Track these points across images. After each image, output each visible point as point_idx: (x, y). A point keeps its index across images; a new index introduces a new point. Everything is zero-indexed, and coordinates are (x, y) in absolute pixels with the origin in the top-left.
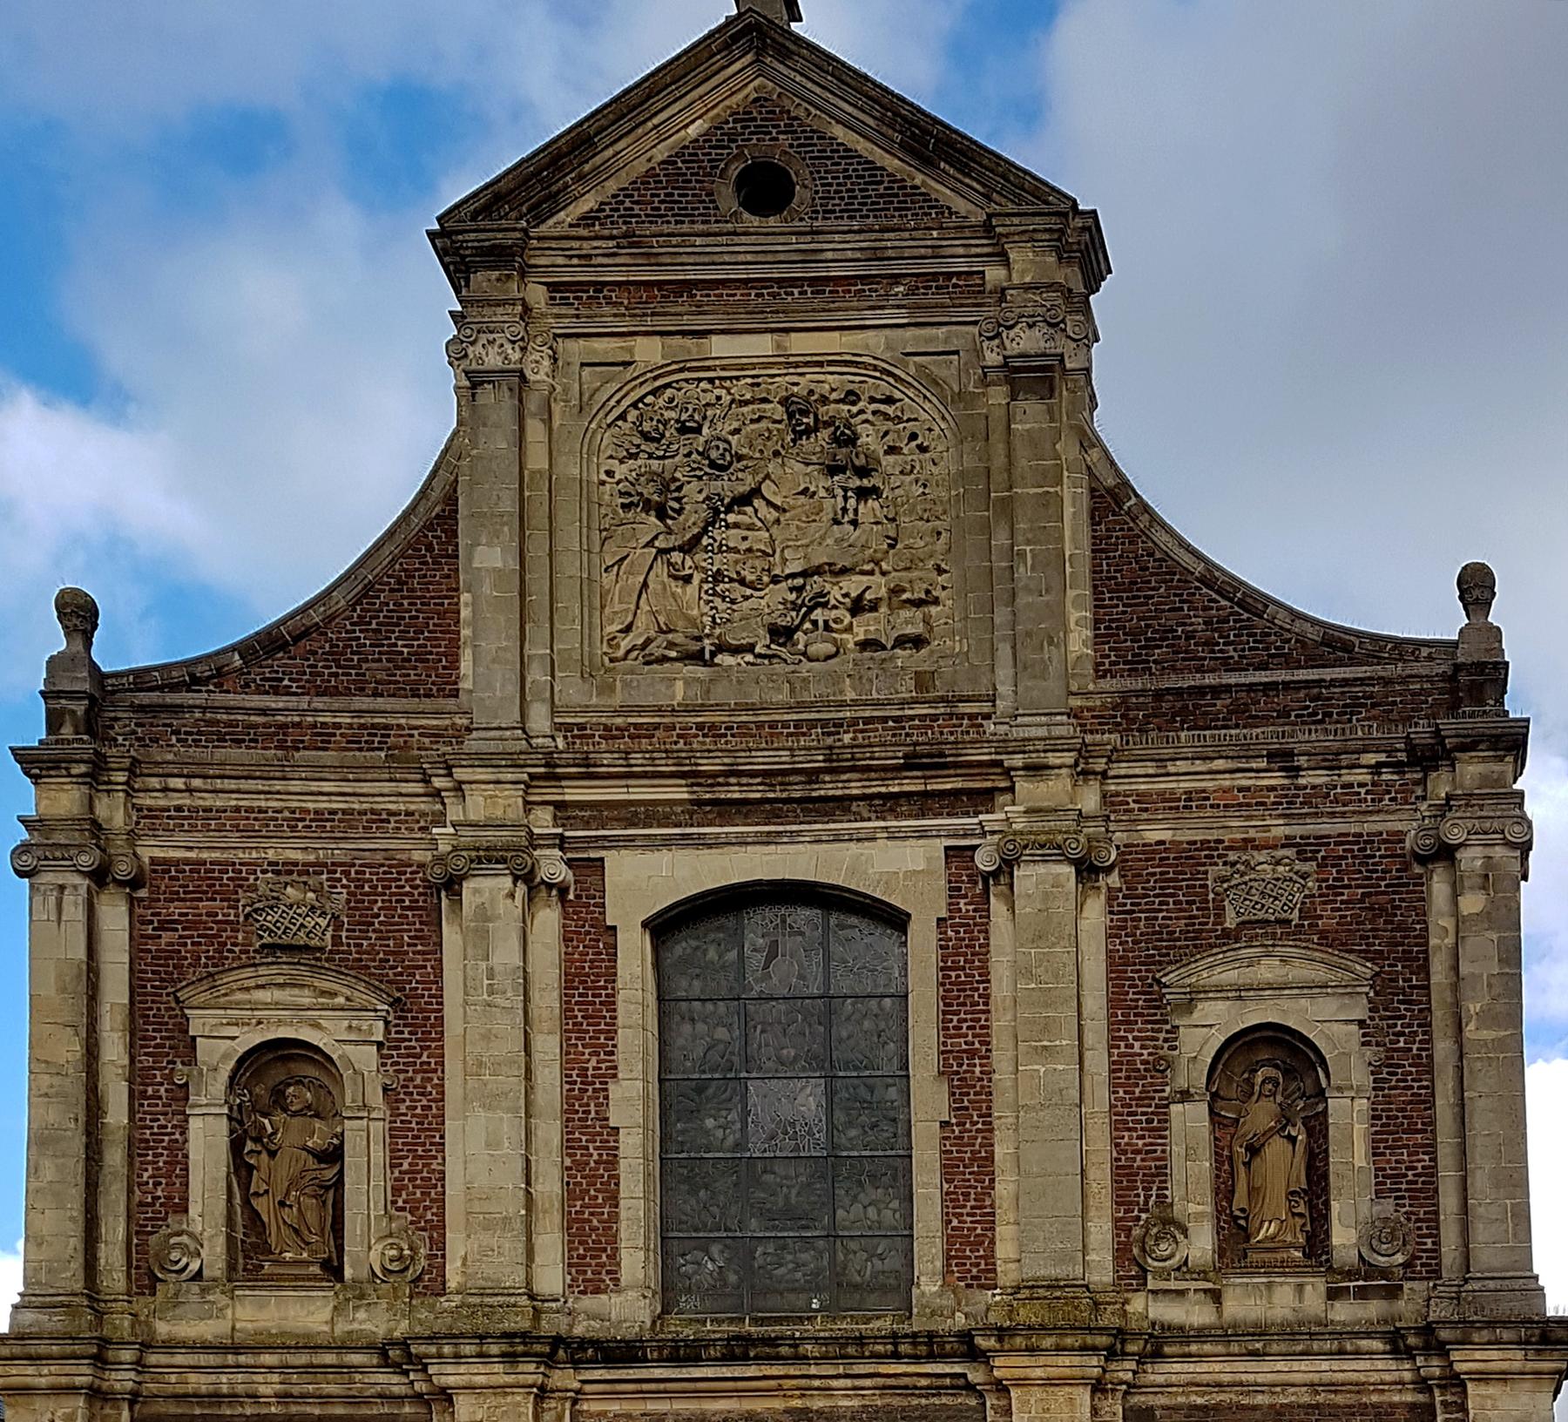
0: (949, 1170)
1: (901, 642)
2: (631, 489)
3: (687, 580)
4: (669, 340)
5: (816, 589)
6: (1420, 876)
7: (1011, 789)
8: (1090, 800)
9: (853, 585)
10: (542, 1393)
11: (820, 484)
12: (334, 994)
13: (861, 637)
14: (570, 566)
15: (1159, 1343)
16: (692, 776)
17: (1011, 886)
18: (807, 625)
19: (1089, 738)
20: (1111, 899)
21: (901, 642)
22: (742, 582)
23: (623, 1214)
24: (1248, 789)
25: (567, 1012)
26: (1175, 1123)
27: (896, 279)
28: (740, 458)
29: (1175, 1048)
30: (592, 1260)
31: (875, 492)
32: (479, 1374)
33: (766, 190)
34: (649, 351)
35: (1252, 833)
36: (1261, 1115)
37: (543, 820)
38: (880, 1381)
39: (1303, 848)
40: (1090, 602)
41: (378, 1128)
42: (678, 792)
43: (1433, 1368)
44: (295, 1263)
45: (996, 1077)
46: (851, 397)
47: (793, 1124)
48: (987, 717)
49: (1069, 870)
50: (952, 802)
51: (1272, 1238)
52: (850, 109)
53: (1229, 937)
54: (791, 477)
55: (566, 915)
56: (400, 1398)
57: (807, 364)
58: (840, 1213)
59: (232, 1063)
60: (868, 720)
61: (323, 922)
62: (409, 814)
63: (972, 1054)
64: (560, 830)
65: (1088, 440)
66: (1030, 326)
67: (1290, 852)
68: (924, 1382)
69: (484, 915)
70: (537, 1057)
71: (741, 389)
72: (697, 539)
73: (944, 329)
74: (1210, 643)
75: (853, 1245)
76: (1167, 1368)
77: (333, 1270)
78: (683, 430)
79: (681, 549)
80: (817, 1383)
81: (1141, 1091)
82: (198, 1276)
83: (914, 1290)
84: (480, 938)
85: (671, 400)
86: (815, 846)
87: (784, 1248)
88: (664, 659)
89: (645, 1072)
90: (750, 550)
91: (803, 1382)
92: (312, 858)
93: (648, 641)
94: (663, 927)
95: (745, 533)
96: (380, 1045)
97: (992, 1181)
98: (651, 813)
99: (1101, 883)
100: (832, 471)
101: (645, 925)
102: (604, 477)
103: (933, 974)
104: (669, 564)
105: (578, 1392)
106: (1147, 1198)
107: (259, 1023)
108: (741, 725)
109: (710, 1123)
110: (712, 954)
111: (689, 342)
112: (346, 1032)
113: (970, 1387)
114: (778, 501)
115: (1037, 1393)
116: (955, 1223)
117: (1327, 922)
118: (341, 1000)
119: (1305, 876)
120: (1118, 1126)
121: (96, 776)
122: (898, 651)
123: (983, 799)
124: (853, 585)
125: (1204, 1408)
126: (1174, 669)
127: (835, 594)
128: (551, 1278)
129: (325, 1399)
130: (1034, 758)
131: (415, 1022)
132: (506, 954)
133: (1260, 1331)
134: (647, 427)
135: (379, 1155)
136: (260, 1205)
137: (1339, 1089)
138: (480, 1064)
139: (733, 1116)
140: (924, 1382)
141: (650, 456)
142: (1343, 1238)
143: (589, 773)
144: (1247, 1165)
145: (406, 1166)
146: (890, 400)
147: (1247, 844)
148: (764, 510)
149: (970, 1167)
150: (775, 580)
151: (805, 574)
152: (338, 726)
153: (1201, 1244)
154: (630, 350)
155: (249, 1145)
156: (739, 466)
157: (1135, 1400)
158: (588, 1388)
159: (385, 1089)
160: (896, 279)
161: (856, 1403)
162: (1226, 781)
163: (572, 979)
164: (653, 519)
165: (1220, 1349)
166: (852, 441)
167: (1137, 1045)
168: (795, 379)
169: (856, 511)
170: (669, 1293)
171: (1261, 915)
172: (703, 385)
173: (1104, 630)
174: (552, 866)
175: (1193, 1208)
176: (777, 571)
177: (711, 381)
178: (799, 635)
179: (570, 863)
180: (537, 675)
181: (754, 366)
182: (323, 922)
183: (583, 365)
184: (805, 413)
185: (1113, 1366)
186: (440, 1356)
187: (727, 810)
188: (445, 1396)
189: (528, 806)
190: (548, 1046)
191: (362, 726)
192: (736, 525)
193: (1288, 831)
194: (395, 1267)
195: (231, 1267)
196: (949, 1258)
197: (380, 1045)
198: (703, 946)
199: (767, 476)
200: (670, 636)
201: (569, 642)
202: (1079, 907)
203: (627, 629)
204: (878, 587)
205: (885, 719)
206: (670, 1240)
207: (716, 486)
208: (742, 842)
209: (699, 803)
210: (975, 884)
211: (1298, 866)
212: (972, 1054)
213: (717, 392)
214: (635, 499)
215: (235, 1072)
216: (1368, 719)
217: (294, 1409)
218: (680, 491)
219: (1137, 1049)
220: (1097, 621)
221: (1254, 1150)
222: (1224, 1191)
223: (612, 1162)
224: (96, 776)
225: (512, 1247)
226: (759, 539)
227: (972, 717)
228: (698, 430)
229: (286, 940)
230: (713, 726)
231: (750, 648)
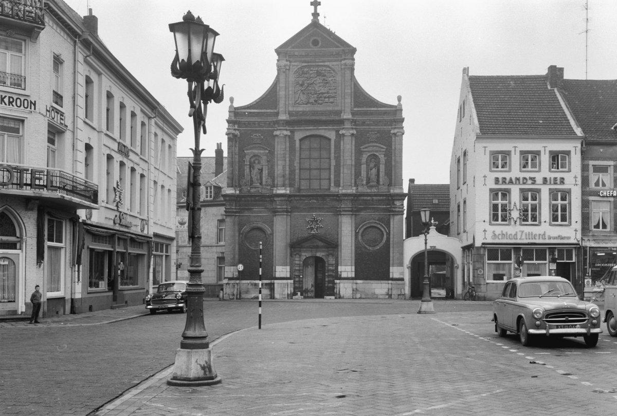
26: (362, 168)
33: (315, 43)
94: (301, 140)
124: (325, 95)
131: (272, 153)
151: (319, 94)
198: (307, 142)
210: (340, 137)
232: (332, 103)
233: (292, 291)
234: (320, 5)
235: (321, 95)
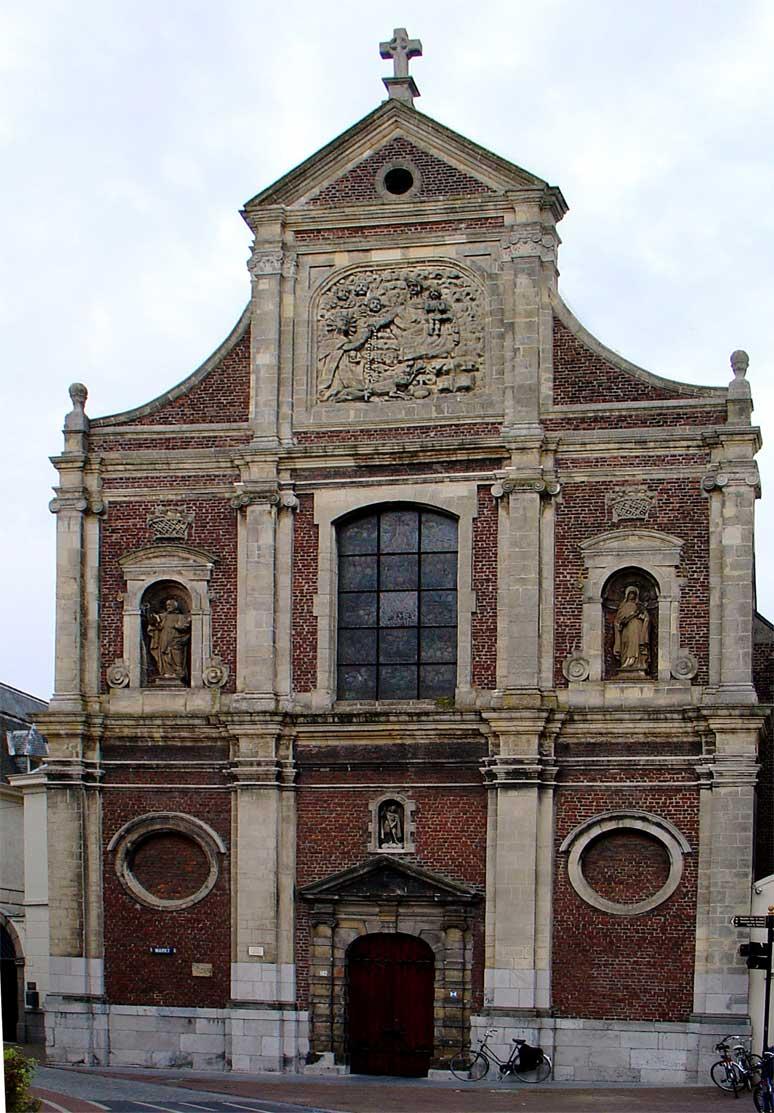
0: (475, 636)
1: (460, 389)
2: (331, 323)
3: (358, 363)
4: (351, 254)
5: (419, 366)
6: (706, 499)
7: (510, 458)
8: (549, 463)
9: (437, 364)
10: (279, 738)
11: (421, 316)
12: (188, 559)
13: (440, 387)
14: (303, 359)
15: (573, 714)
16: (355, 455)
17: (508, 503)
18: (415, 382)
19: (550, 434)
20: (558, 508)
21: (460, 389)
22: (384, 363)
23: (319, 655)
24: (625, 457)
25: (295, 564)
27: (460, 221)
28: (385, 306)
29: (586, 578)
30: (304, 678)
31: (448, 320)
32: (249, 729)
33: (399, 182)
34: (342, 260)
35: (627, 478)
36: (628, 609)
37: (286, 478)
38: (439, 732)
39: (652, 485)
40: (552, 370)
41: (207, 619)
42: (350, 463)
43: (701, 726)
44: (170, 679)
45: (499, 591)
46: (438, 277)
47: (401, 613)
48: (500, 423)
49: (537, 496)
50: (482, 464)
51: (631, 666)
52: (440, 142)
53: (615, 526)
54: (411, 312)
55: (295, 520)
56: (215, 739)
57: (418, 262)
58: (423, 654)
59: (142, 592)
60: (441, 426)
61: (184, 527)
62: (224, 476)
63: (488, 580)
64: (293, 482)
65: (552, 293)
66: (525, 243)
67: (645, 487)
68: (459, 732)
69: (257, 522)
70: (280, 586)
71: (386, 275)
72: (363, 344)
73: (483, 244)
74: (610, 388)
75: (429, 668)
76: (576, 726)
77: (186, 681)
78: (357, 295)
79: (355, 350)
80: (408, 733)
81: (569, 598)
82: (127, 686)
83: (457, 691)
84: (255, 533)
85: (352, 281)
86: (415, 486)
87: (396, 669)
88: (346, 400)
89: (331, 590)
90: (388, 349)
91: (402, 732)
92: (179, 498)
93: (338, 392)
94: (341, 524)
95: (385, 341)
96: (208, 581)
97: (496, 640)
98: (338, 472)
99: (553, 501)
100: (429, 312)
101: (332, 523)
102: (319, 318)
103: (470, 544)
104: (349, 357)
105: (296, 736)
106: (571, 647)
107: (155, 573)
108: (381, 430)
109: (362, 612)
110: (365, 535)
111: (361, 254)
112: (191, 575)
113: (482, 735)
114: (402, 326)
115: (512, 738)
116: (477, 659)
117: (663, 519)
118: (191, 561)
119: (651, 498)
120: (558, 613)
121: (86, 467)
122: (458, 393)
123: (497, 463)
124: (437, 364)
125: (593, 744)
126: (591, 400)
127: (429, 368)
128: (285, 684)
129: (183, 739)
130: (520, 445)
131: (224, 573)
132: (267, 538)
133: (619, 709)
134: (340, 294)
135: (207, 630)
136: (154, 653)
137: (665, 597)
138: (253, 590)
139: (374, 609)
141: (342, 307)
142: (663, 665)
143: (307, 455)
144: (621, 632)
145: (219, 635)
146: (457, 277)
147: (623, 483)
148: (395, 330)
149: (486, 634)
150: (400, 362)
151: (413, 359)
152: (193, 438)
153: (596, 668)
154: (333, 260)
155: (150, 627)
156: (383, 310)
157: (561, 740)
159: (210, 601)
160: (460, 221)
161: (427, 741)
162: (616, 453)
163: (297, 548)
164: (342, 337)
165: (600, 717)
166: (439, 297)
167: (568, 576)
168: (412, 269)
169: (440, 330)
170: (341, 693)
171: (630, 516)
172: (368, 273)
173: (559, 383)
174: (289, 498)
175: (592, 652)
176: (400, 358)
177: (372, 271)
178: (411, 387)
179: (297, 496)
180: (286, 410)
181: (391, 264)
182: (184, 527)
183: (311, 267)
184: (416, 286)
185: (550, 726)
186: (233, 721)
187: (373, 470)
188: (236, 738)
189: (279, 471)
190: (286, 580)
191: (204, 437)
192: (382, 338)
193: (645, 477)
194: (214, 681)
195: (142, 682)
196: (474, 675)
197: (208, 581)
198: (364, 533)
199: (397, 315)
200: (350, 390)
201: (301, 395)
202: (541, 512)
203: (329, 387)
204: (450, 364)
205: (451, 425)
206: (342, 665)
207: (371, 321)
208: (380, 484)
209: (360, 467)
210: (490, 504)
211: (650, 494)
212: (488, 580)
213: (374, 276)
214: (334, 327)
215: (144, 594)
216: (684, 425)
217: (170, 743)
218: (355, 326)
219: (568, 578)
220: (555, 379)
221: (624, 625)
222: (608, 643)
223: (314, 633)
224: (86, 467)
225: (267, 671)
226: (393, 343)
227: (493, 424)
228: (365, 295)
229: (167, 536)
230: (368, 431)
231: (387, 394)
232: (467, 389)
233: (305, 1050)
234: (417, 52)
235: (419, 364)
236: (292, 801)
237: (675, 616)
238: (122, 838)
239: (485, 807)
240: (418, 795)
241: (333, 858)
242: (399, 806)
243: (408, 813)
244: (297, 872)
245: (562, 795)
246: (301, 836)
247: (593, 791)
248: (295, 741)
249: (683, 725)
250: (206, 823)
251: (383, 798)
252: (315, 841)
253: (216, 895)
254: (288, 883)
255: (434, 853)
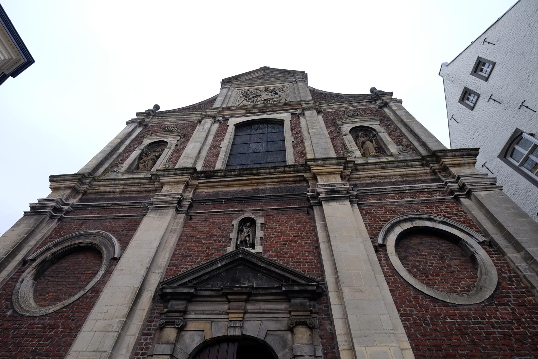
38: (279, 180)
94: (238, 126)
101: (234, 125)
105: (197, 186)
140: (291, 179)
158: (200, 185)
223: (219, 152)
236: (182, 220)
237: (388, 137)
238: (48, 249)
239: (313, 219)
240: (265, 214)
241: (199, 260)
242: (252, 222)
243: (258, 225)
244: (167, 272)
245: (363, 209)
246: (178, 245)
247: (384, 206)
248: (196, 189)
249: (423, 169)
250: (116, 238)
251: (243, 217)
252: (188, 248)
253: (87, 298)
254: (155, 280)
255: (277, 252)
